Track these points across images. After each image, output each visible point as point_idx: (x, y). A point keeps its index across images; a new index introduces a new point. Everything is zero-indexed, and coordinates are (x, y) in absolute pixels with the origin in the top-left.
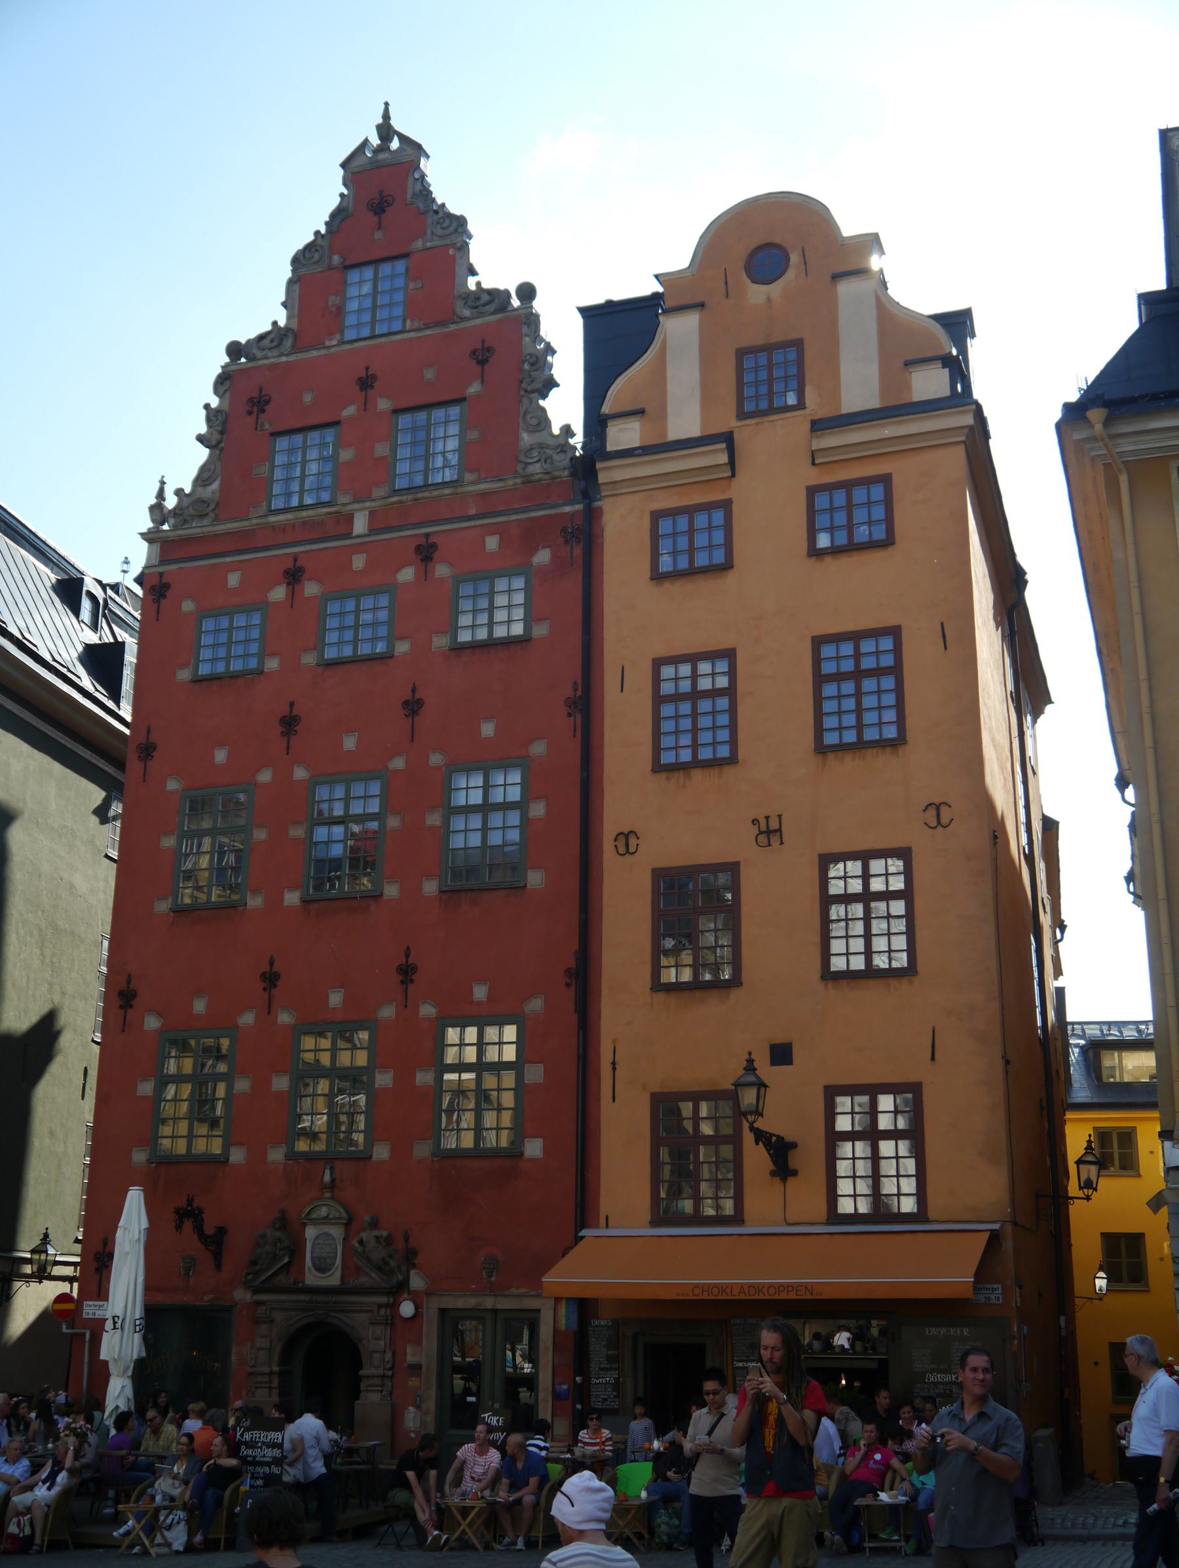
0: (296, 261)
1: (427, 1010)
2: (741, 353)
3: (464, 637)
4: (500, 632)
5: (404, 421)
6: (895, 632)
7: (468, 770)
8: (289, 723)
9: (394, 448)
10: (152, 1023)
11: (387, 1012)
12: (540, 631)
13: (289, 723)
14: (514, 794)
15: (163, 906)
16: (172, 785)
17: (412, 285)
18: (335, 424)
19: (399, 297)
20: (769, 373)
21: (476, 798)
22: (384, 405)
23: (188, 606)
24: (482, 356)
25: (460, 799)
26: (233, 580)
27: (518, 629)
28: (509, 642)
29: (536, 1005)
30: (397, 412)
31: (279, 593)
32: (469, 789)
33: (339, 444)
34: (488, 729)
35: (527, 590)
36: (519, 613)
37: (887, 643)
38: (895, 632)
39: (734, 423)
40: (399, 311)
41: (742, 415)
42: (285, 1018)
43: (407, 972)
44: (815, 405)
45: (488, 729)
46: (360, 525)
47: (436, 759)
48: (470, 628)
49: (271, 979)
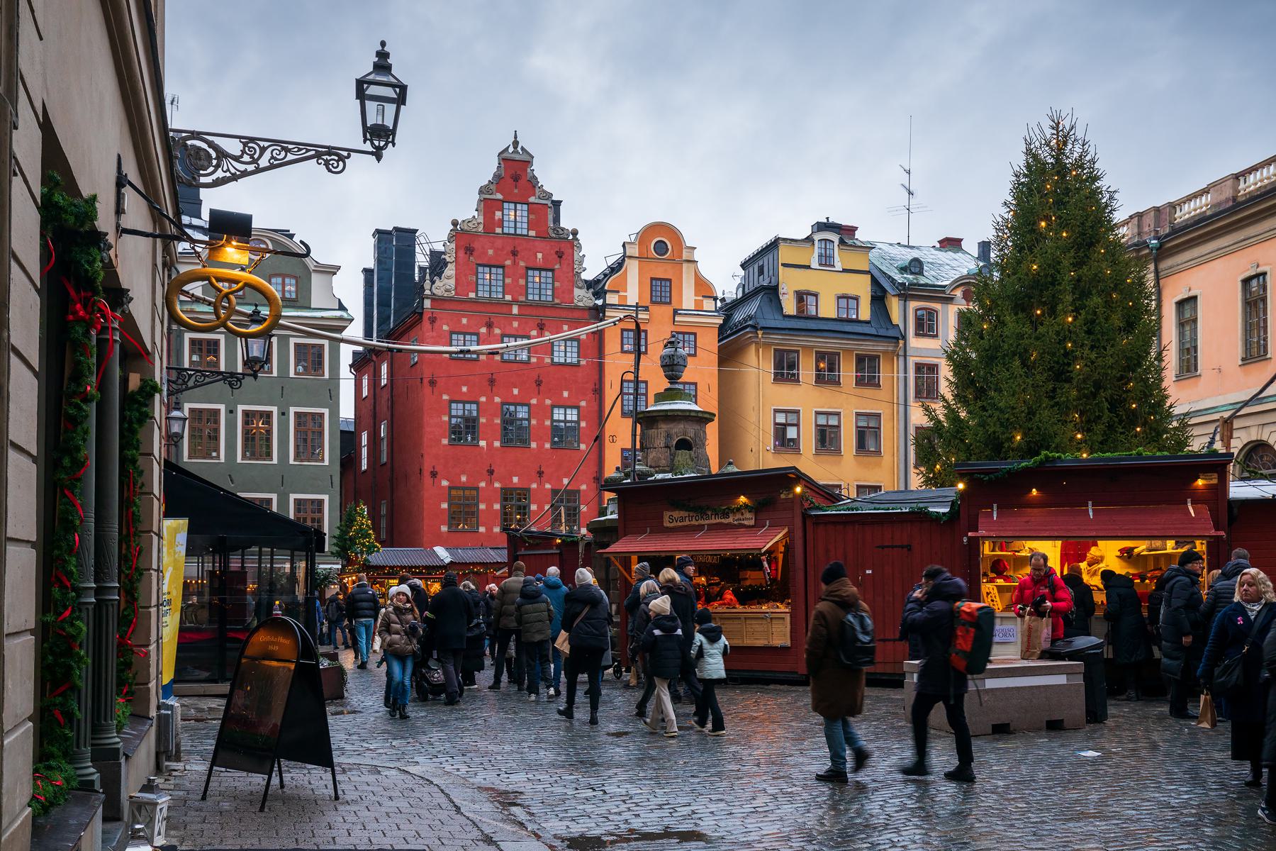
0: (481, 192)
1: (548, 486)
2: (652, 279)
3: (556, 360)
4: (569, 360)
5: (530, 273)
6: (696, 384)
7: (559, 407)
8: (492, 382)
9: (527, 282)
10: (445, 483)
11: (534, 486)
12: (583, 362)
13: (492, 382)
14: (575, 418)
15: (445, 441)
16: (445, 397)
17: (532, 217)
18: (503, 267)
19: (525, 220)
20: (661, 291)
21: (562, 418)
22: (522, 264)
23: (445, 328)
24: (560, 255)
25: (556, 417)
26: (464, 321)
27: (575, 361)
28: (571, 365)
29: (584, 487)
30: (528, 268)
31: (483, 330)
32: (558, 414)
33: (504, 276)
34: (566, 394)
35: (579, 347)
36: (575, 355)
37: (693, 387)
38: (696, 384)
39: (648, 304)
40: (525, 226)
41: (652, 302)
42: (497, 485)
43: (540, 474)
44: (675, 305)
45: (566, 394)
46: (515, 310)
47: (548, 402)
48: (559, 357)
49: (491, 472)
